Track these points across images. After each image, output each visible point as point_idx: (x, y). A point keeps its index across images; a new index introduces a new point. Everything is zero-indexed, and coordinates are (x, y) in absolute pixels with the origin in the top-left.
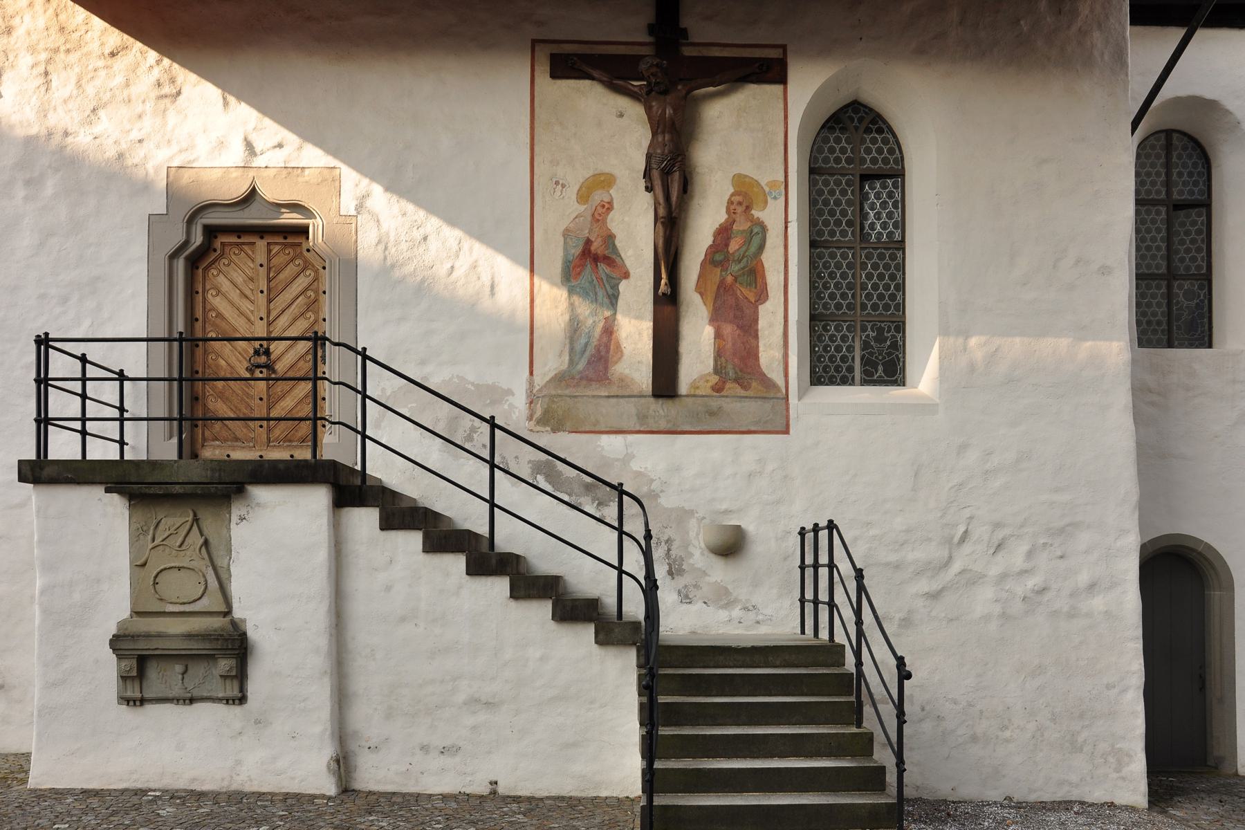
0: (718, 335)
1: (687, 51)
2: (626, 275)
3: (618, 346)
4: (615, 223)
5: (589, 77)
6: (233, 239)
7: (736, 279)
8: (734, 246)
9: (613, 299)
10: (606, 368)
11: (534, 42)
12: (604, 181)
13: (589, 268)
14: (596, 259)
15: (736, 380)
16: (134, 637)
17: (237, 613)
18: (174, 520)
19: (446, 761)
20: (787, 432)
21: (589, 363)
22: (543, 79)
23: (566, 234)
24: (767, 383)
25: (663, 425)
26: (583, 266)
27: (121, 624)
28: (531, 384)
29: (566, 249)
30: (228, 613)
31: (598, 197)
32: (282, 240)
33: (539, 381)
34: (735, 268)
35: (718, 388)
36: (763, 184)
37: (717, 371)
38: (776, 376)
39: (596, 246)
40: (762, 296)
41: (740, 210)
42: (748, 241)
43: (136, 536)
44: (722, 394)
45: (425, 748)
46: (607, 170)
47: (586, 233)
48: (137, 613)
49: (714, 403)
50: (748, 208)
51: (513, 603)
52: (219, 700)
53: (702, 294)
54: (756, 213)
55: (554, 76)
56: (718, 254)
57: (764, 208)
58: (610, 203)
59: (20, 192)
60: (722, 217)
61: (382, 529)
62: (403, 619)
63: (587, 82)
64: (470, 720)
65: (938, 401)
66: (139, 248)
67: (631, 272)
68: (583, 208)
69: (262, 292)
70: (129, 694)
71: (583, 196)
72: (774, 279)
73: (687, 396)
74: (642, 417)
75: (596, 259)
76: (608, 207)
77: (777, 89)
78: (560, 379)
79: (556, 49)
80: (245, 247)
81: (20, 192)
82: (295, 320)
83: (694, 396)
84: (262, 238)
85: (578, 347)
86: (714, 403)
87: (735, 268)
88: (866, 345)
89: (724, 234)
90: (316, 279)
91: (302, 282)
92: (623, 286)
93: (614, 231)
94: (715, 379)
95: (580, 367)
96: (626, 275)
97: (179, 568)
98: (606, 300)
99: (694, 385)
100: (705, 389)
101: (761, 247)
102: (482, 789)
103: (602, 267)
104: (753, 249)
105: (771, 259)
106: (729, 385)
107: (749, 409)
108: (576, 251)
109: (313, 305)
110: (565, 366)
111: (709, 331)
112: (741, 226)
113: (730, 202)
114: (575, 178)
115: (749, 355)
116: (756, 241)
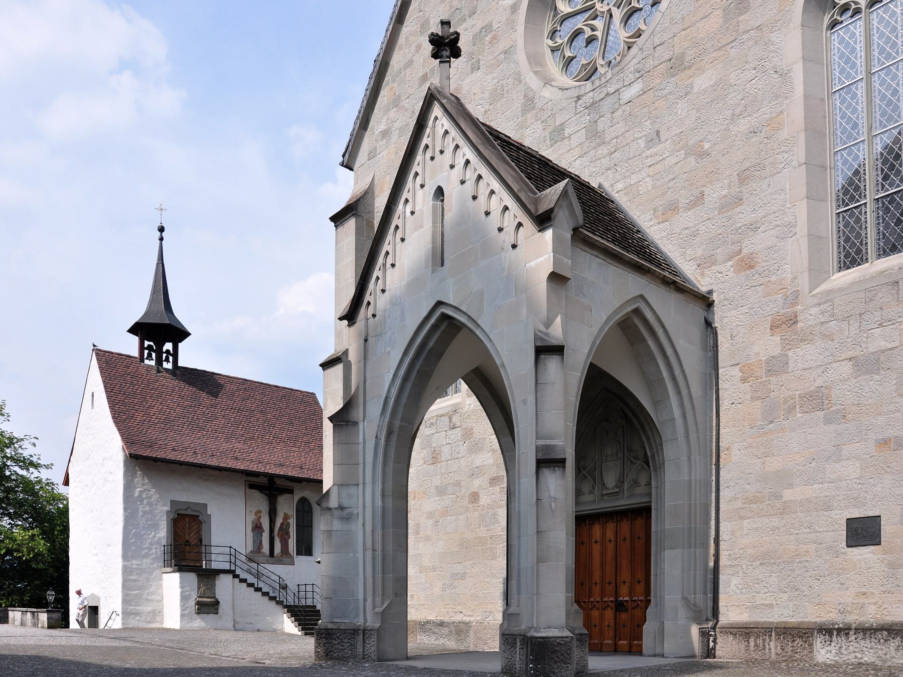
1: (275, 486)
2: (264, 532)
3: (263, 547)
4: (262, 520)
8: (284, 527)
9: (262, 536)
10: (260, 550)
14: (258, 528)
15: (285, 554)
21: (257, 549)
22: (247, 489)
25: (271, 562)
26: (256, 529)
30: (215, 597)
31: (259, 515)
33: (248, 552)
34: (284, 532)
35: (282, 556)
37: (281, 552)
39: (258, 525)
40: (289, 538)
49: (281, 559)
52: (214, 613)
53: (278, 536)
54: (288, 521)
55: (249, 488)
56: (281, 529)
63: (255, 490)
72: (291, 534)
74: (267, 561)
75: (258, 528)
77: (292, 495)
78: (251, 552)
82: (194, 535)
85: (255, 546)
86: (281, 559)
88: (305, 547)
89: (282, 524)
90: (199, 526)
94: (281, 554)
95: (255, 549)
96: (264, 532)
99: (277, 555)
101: (289, 528)
103: (259, 529)
105: (291, 530)
106: (284, 555)
108: (254, 526)
111: (280, 544)
112: (285, 523)
113: (283, 518)
114: (254, 511)
115: (288, 549)
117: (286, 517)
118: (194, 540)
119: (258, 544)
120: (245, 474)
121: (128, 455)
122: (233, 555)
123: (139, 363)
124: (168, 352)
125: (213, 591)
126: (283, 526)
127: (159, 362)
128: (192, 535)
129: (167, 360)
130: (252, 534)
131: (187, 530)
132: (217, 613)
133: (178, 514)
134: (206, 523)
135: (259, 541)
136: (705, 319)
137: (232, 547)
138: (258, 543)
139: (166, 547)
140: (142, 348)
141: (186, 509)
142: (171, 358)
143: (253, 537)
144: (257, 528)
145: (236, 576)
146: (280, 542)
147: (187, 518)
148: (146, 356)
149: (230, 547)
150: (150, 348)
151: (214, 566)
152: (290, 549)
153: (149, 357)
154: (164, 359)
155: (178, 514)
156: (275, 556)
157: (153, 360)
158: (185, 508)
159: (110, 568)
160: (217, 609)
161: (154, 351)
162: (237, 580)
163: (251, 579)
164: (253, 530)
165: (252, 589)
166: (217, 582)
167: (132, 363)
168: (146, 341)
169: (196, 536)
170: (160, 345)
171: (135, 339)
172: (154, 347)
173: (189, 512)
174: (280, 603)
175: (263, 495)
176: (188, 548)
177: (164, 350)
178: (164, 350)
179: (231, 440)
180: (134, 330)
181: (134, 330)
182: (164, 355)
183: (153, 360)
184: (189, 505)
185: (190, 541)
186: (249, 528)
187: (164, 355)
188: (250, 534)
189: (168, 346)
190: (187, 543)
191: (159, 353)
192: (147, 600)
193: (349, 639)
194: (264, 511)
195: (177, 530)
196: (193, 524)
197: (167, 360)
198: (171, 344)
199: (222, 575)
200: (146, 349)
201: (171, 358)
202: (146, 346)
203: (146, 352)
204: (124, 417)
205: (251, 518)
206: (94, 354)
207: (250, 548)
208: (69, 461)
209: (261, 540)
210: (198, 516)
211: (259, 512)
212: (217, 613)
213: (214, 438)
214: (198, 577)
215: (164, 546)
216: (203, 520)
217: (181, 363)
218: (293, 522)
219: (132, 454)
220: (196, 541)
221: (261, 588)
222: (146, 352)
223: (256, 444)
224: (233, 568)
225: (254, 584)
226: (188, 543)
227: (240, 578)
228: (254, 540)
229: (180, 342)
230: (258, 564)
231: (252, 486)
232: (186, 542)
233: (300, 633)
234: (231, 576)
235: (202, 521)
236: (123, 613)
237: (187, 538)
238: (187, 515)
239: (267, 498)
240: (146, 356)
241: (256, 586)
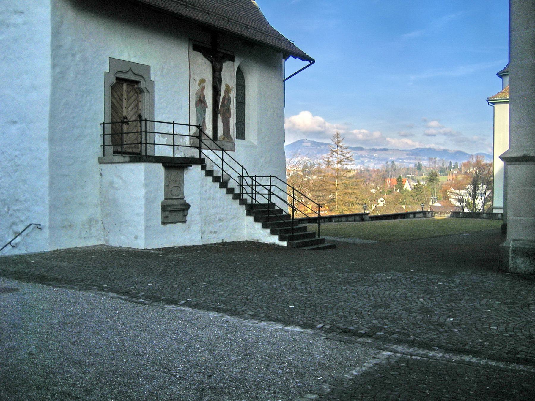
0: (224, 125)
2: (207, 107)
3: (206, 126)
7: (226, 111)
8: (225, 102)
9: (205, 112)
12: (202, 81)
16: (167, 206)
18: (174, 173)
19: (215, 235)
20: (234, 151)
23: (196, 94)
24: (231, 138)
27: (162, 203)
29: (196, 99)
31: (202, 85)
32: (130, 84)
35: (224, 139)
36: (230, 87)
37: (224, 134)
38: (232, 137)
39: (202, 97)
41: (227, 93)
42: (228, 102)
43: (166, 177)
44: (225, 140)
45: (211, 232)
46: (203, 78)
48: (166, 199)
50: (228, 93)
51: (226, 194)
57: (230, 94)
58: (204, 87)
59: (70, 58)
60: (224, 95)
62: (208, 199)
64: (218, 225)
65: (257, 145)
66: (102, 82)
67: (208, 106)
68: (199, 87)
69: (125, 99)
70: (165, 221)
71: (199, 85)
72: (232, 111)
73: (218, 141)
76: (203, 88)
79: (196, 43)
80: (121, 85)
81: (70, 58)
82: (133, 109)
83: (220, 140)
84: (125, 82)
87: (226, 108)
89: (224, 98)
90: (138, 97)
92: (207, 109)
93: (205, 94)
94: (223, 136)
97: (176, 186)
98: (203, 113)
100: (222, 140)
101: (230, 104)
102: (220, 241)
103: (203, 104)
104: (229, 103)
106: (225, 138)
107: (227, 145)
108: (198, 99)
109: (137, 105)
111: (222, 124)
112: (227, 97)
113: (225, 90)
114: (198, 79)
116: (229, 101)
117: (228, 90)
118: (132, 116)
126: (224, 101)
128: (130, 109)
130: (195, 109)
131: (125, 102)
132: (185, 222)
133: (117, 79)
134: (149, 92)
143: (197, 114)
144: (201, 101)
145: (204, 167)
146: (222, 122)
147: (125, 87)
152: (231, 131)
155: (117, 79)
156: (218, 139)
158: (124, 70)
159: (16, 156)
160: (185, 216)
169: (135, 110)
173: (129, 76)
174: (243, 202)
176: (125, 127)
184: (130, 66)
185: (129, 117)
186: (193, 103)
188: (194, 109)
190: (125, 121)
192: (81, 204)
194: (207, 82)
195: (114, 101)
196: (132, 93)
205: (196, 87)
209: (204, 118)
210: (137, 82)
211: (202, 81)
212: (185, 222)
214: (165, 170)
216: (146, 88)
218: (233, 95)
226: (125, 120)
228: (197, 117)
233: (285, 244)
234: (199, 167)
235: (145, 90)
236: (50, 228)
237: (125, 114)
239: (210, 64)
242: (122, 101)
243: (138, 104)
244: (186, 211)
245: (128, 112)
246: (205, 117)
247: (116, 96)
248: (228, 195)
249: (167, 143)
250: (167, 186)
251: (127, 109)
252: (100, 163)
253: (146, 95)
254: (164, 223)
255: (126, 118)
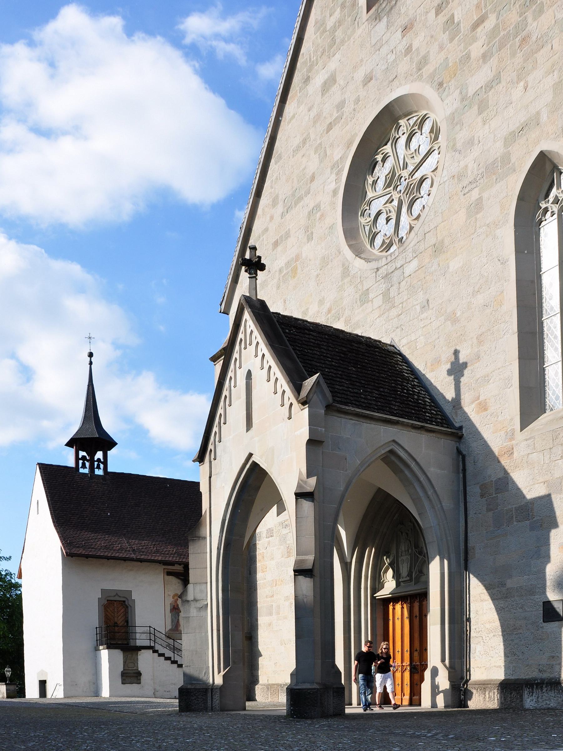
2: (181, 612)
5: (174, 576)
6: (110, 602)
11: (164, 569)
13: (174, 611)
16: (124, 673)
17: (139, 670)
19: (168, 693)
21: (175, 627)
23: (170, 604)
27: (122, 672)
28: (165, 631)
33: (167, 630)
45: (165, 691)
47: (174, 604)
48: (124, 670)
61: (158, 656)
68: (173, 600)
70: (124, 682)
71: (173, 598)
78: (170, 630)
85: (173, 625)
91: (123, 610)
103: (177, 610)
110: (171, 628)
119: (176, 624)
120: (162, 564)
121: (65, 554)
122: (152, 633)
123: (75, 472)
124: (99, 460)
125: (136, 664)
127: (92, 468)
128: (120, 617)
129: (98, 467)
131: (116, 613)
132: (140, 683)
133: (107, 600)
135: (177, 620)
136: (457, 449)
137: (151, 627)
138: (176, 622)
139: (98, 629)
140: (77, 459)
141: (115, 596)
142: (102, 466)
143: (172, 617)
145: (155, 651)
148: (80, 465)
149: (150, 627)
150: (84, 458)
151: (139, 643)
153: (84, 466)
154: (96, 466)
155: (107, 600)
157: (87, 468)
161: (88, 461)
162: (156, 654)
163: (168, 653)
164: (172, 611)
165: (169, 662)
166: (140, 657)
167: (70, 472)
168: (80, 451)
169: (123, 618)
170: (92, 454)
171: (71, 451)
172: (87, 457)
175: (179, 581)
176: (116, 628)
177: (96, 459)
178: (96, 459)
179: (151, 534)
180: (70, 444)
181: (70, 444)
182: (96, 463)
183: (87, 468)
187: (96, 463)
188: (169, 614)
189: (99, 455)
190: (116, 624)
191: (92, 461)
193: (202, 696)
195: (108, 613)
197: (98, 467)
198: (102, 452)
199: (143, 651)
200: (81, 459)
201: (102, 466)
202: (80, 457)
203: (81, 462)
204: (62, 521)
205: (170, 600)
206: (38, 466)
207: (169, 627)
208: (22, 558)
209: (178, 620)
210: (124, 601)
212: (140, 683)
213: (137, 533)
214: (123, 653)
215: (97, 628)
217: (110, 469)
219: (68, 553)
220: (123, 623)
221: (177, 661)
222: (81, 462)
223: (174, 536)
224: (152, 645)
225: (171, 658)
227: (159, 653)
228: (172, 619)
229: (110, 450)
230: (174, 641)
231: (169, 573)
232: (115, 623)
234: (151, 651)
237: (116, 620)
238: (115, 601)
240: (80, 465)
241: (172, 659)
242: (114, 614)
243: (125, 614)
244: (139, 678)
245: (120, 621)
246: (179, 619)
247: (109, 611)
248: (179, 668)
249: (146, 638)
250: (125, 662)
251: (118, 618)
252: (96, 650)
253: (129, 608)
254: (123, 683)
255: (117, 623)
